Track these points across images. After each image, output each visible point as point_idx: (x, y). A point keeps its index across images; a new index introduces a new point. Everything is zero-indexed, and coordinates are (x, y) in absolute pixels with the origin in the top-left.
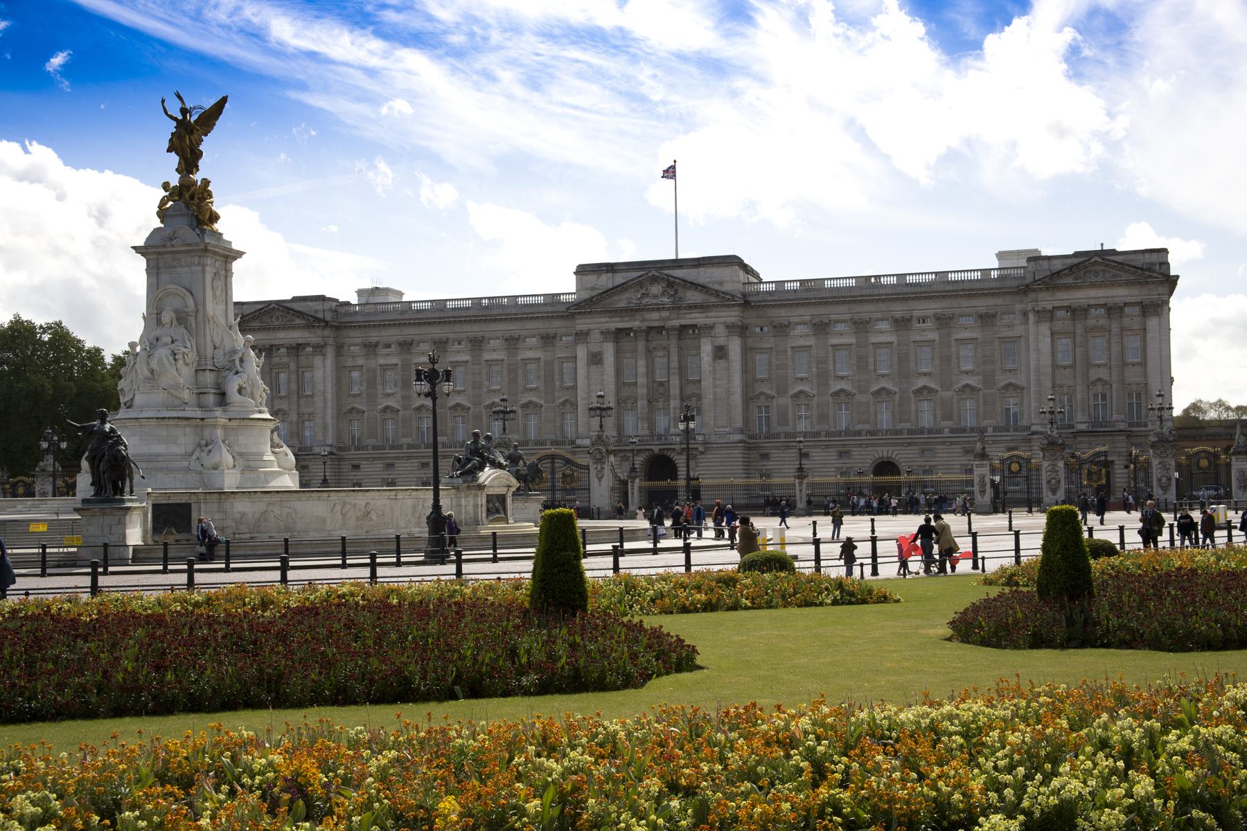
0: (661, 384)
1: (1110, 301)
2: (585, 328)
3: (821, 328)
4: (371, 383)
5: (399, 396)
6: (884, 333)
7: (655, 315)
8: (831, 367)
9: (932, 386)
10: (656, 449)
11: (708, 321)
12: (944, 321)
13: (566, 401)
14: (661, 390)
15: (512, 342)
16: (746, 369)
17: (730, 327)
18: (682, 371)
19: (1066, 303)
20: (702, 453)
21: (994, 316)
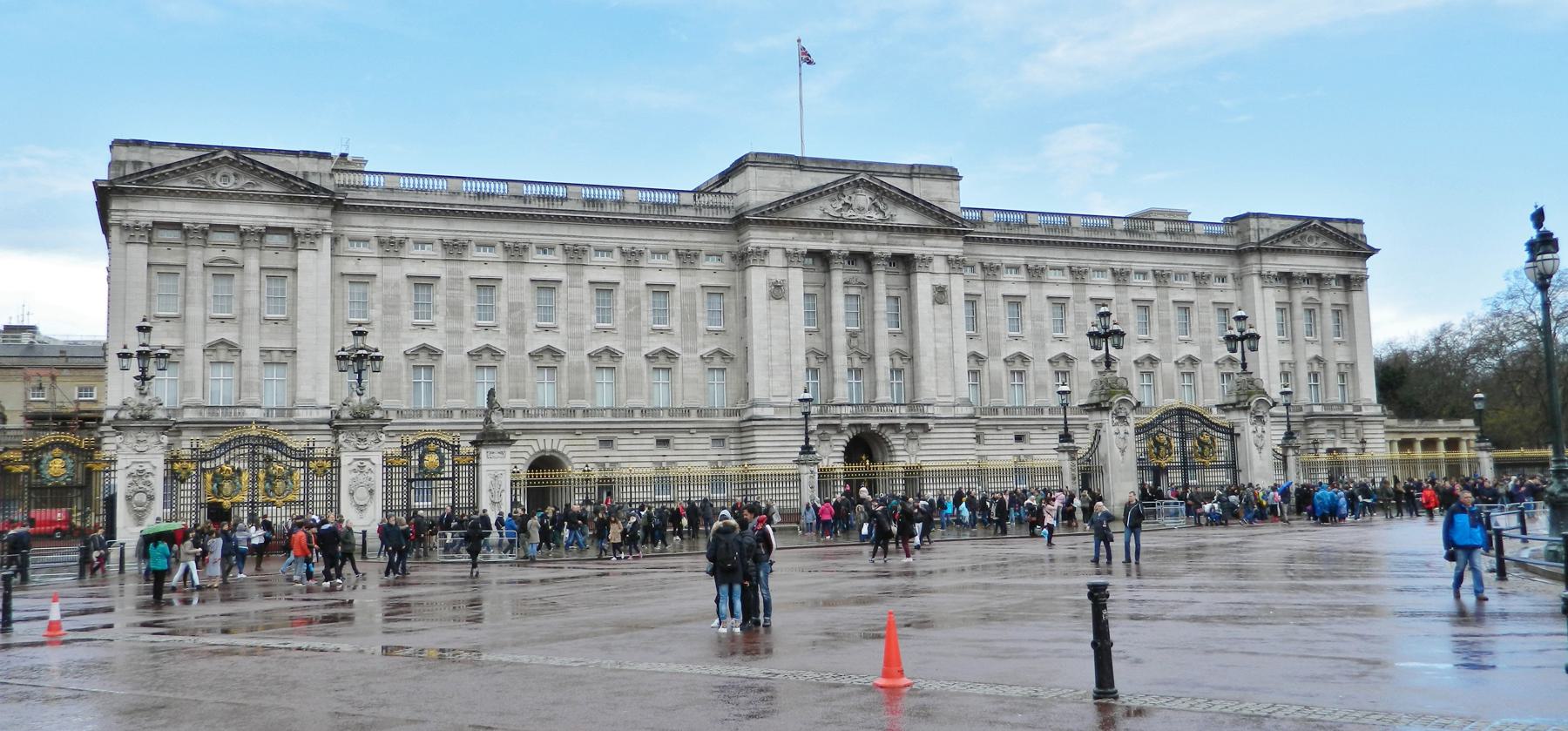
1: (1324, 271)
2: (763, 243)
3: (1035, 274)
4: (391, 307)
5: (441, 329)
6: (1102, 287)
7: (858, 236)
8: (1048, 324)
9: (1156, 354)
12: (1161, 277)
13: (719, 352)
14: (854, 343)
15: (632, 257)
17: (949, 261)
19: (1287, 269)
21: (1209, 277)
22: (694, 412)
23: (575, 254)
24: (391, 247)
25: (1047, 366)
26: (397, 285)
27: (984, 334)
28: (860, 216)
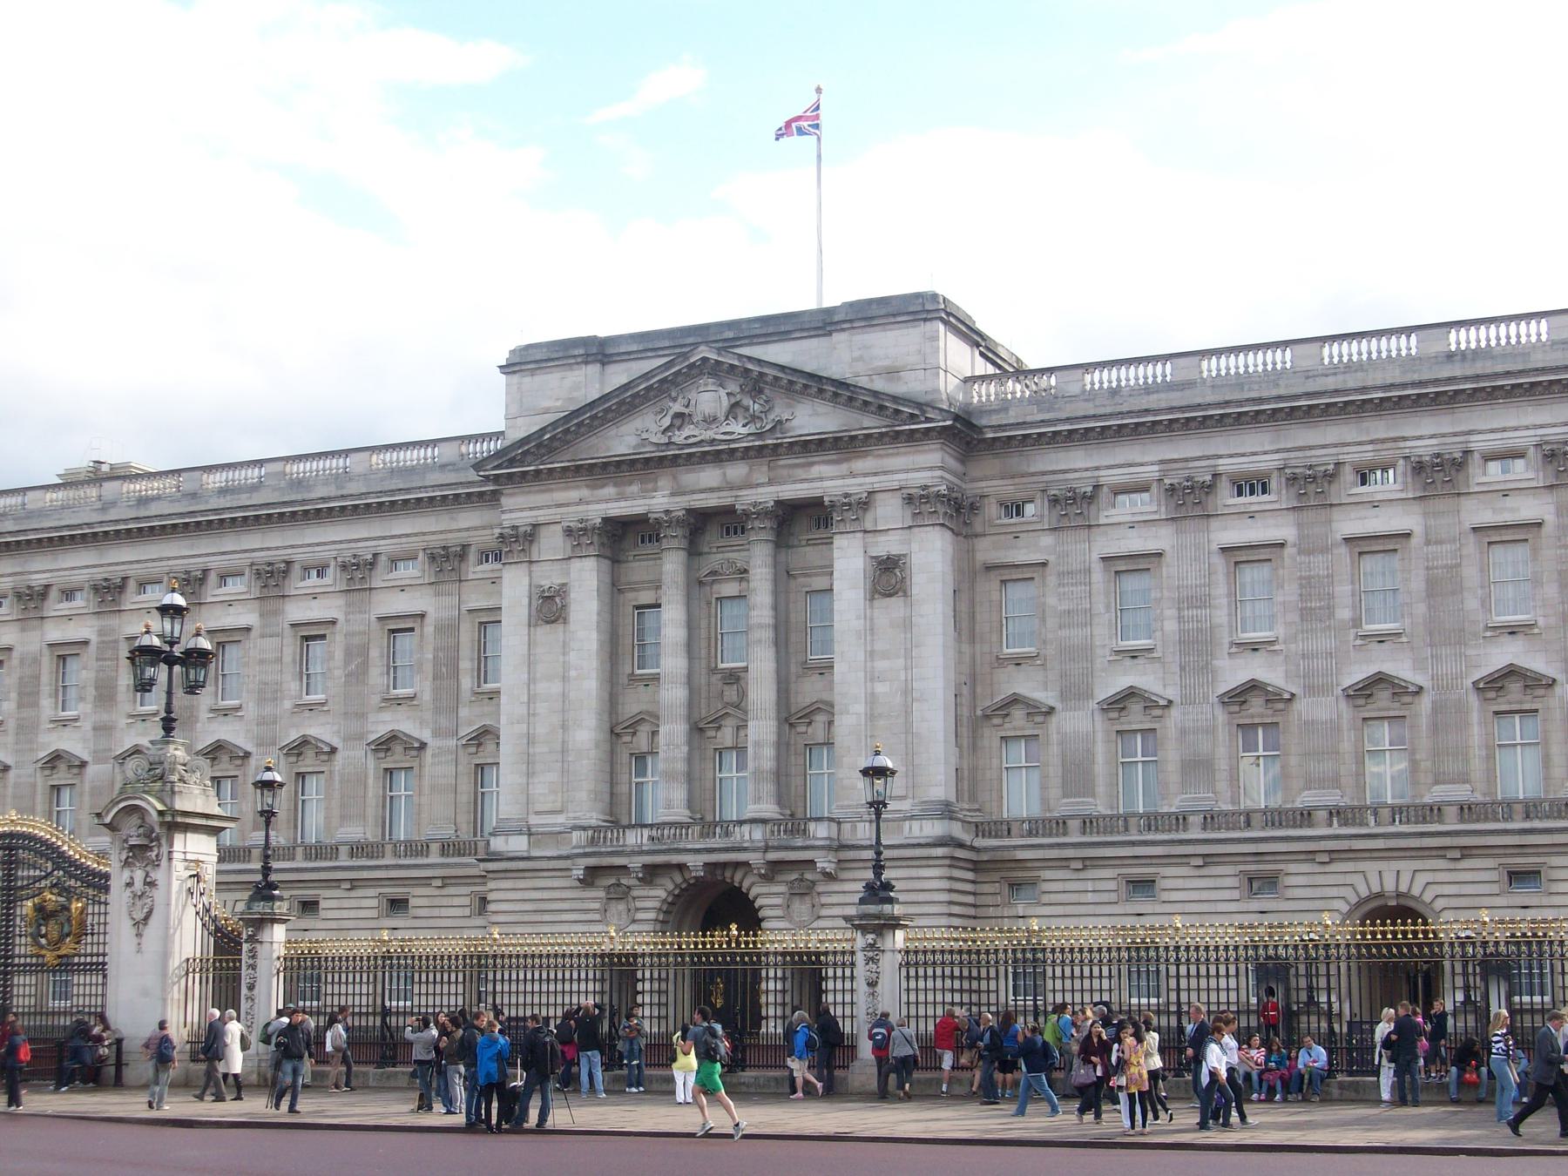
0: (734, 678)
2: (523, 518)
3: (1189, 498)
5: (87, 725)
6: (1385, 506)
7: (709, 476)
8: (1221, 616)
9: (1537, 663)
10: (695, 862)
11: (856, 487)
14: (731, 694)
16: (967, 624)
17: (918, 502)
18: (783, 635)
20: (829, 877)
22: (435, 847)
23: (272, 579)
24: (32, 599)
25: (1221, 716)
26: (36, 661)
27: (1050, 651)
28: (709, 435)
